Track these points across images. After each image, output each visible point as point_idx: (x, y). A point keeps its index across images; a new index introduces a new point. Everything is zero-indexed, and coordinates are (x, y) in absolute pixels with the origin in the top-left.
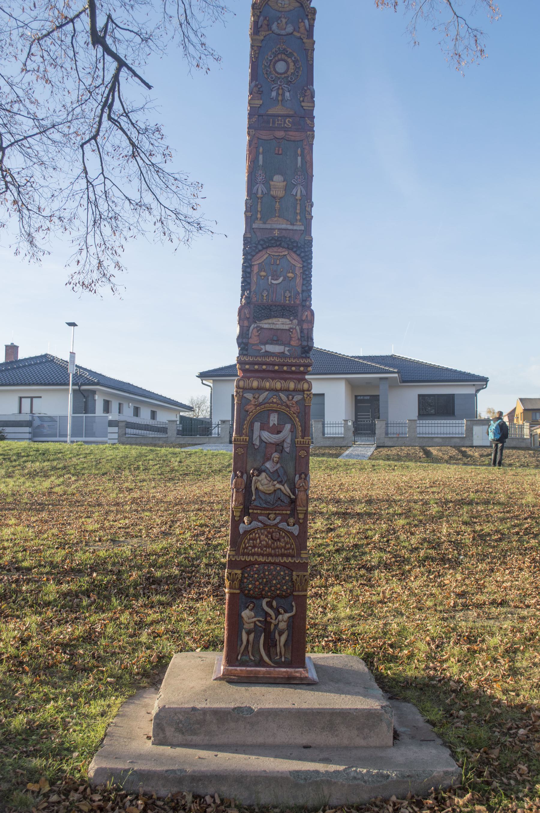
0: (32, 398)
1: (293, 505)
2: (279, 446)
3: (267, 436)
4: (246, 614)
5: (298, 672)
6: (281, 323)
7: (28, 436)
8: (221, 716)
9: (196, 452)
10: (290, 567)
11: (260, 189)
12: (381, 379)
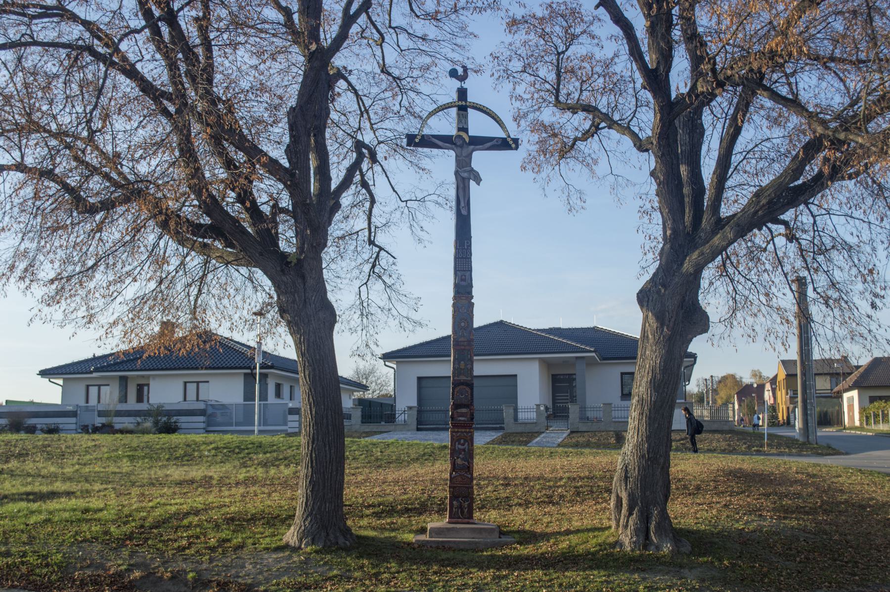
0: (198, 383)
1: (469, 468)
2: (464, 450)
3: (460, 446)
4: (455, 502)
5: (471, 521)
6: (464, 410)
7: (202, 425)
8: (448, 529)
9: (393, 443)
10: (468, 488)
11: (457, 366)
12: (577, 358)
